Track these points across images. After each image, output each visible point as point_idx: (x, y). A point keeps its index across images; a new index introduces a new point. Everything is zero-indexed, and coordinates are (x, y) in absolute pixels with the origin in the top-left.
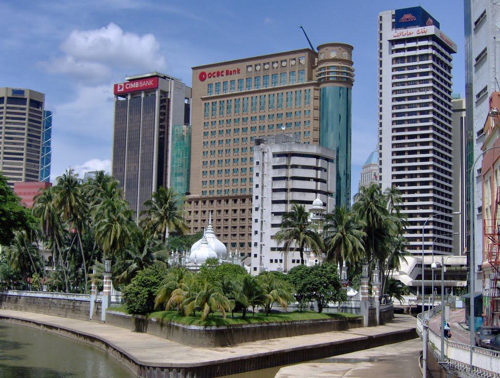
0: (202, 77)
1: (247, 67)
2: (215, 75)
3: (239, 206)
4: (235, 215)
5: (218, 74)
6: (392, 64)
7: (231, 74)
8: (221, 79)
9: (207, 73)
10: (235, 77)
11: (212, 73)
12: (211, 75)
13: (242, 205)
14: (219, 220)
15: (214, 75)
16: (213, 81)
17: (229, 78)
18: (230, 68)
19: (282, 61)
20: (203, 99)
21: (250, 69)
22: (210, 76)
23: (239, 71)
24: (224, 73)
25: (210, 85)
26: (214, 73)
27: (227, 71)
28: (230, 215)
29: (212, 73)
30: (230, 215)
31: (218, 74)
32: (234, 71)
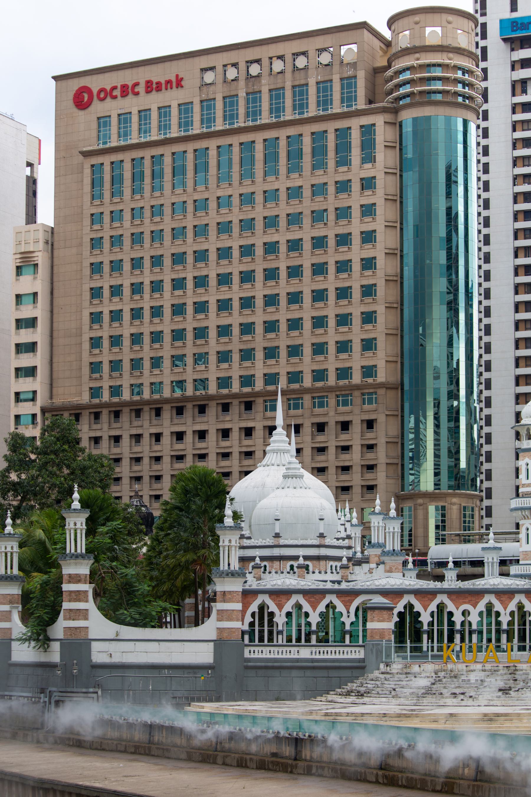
0: (82, 100)
1: (204, 70)
2: (117, 93)
3: (189, 424)
4: (202, 445)
5: (125, 91)
6: (514, 95)
7: (159, 88)
8: (132, 105)
9: (95, 92)
10: (173, 98)
11: (108, 88)
12: (106, 94)
13: (221, 418)
14: (138, 460)
15: (115, 93)
16: (112, 108)
17: (153, 101)
18: (158, 74)
19: (296, 55)
20: (86, 154)
21: (209, 77)
22: (102, 95)
23: (179, 82)
24: (141, 89)
25: (103, 121)
26: (114, 88)
27: (149, 83)
28: (167, 446)
29: (108, 88)
30: (167, 446)
31: (125, 91)
32: (169, 82)
